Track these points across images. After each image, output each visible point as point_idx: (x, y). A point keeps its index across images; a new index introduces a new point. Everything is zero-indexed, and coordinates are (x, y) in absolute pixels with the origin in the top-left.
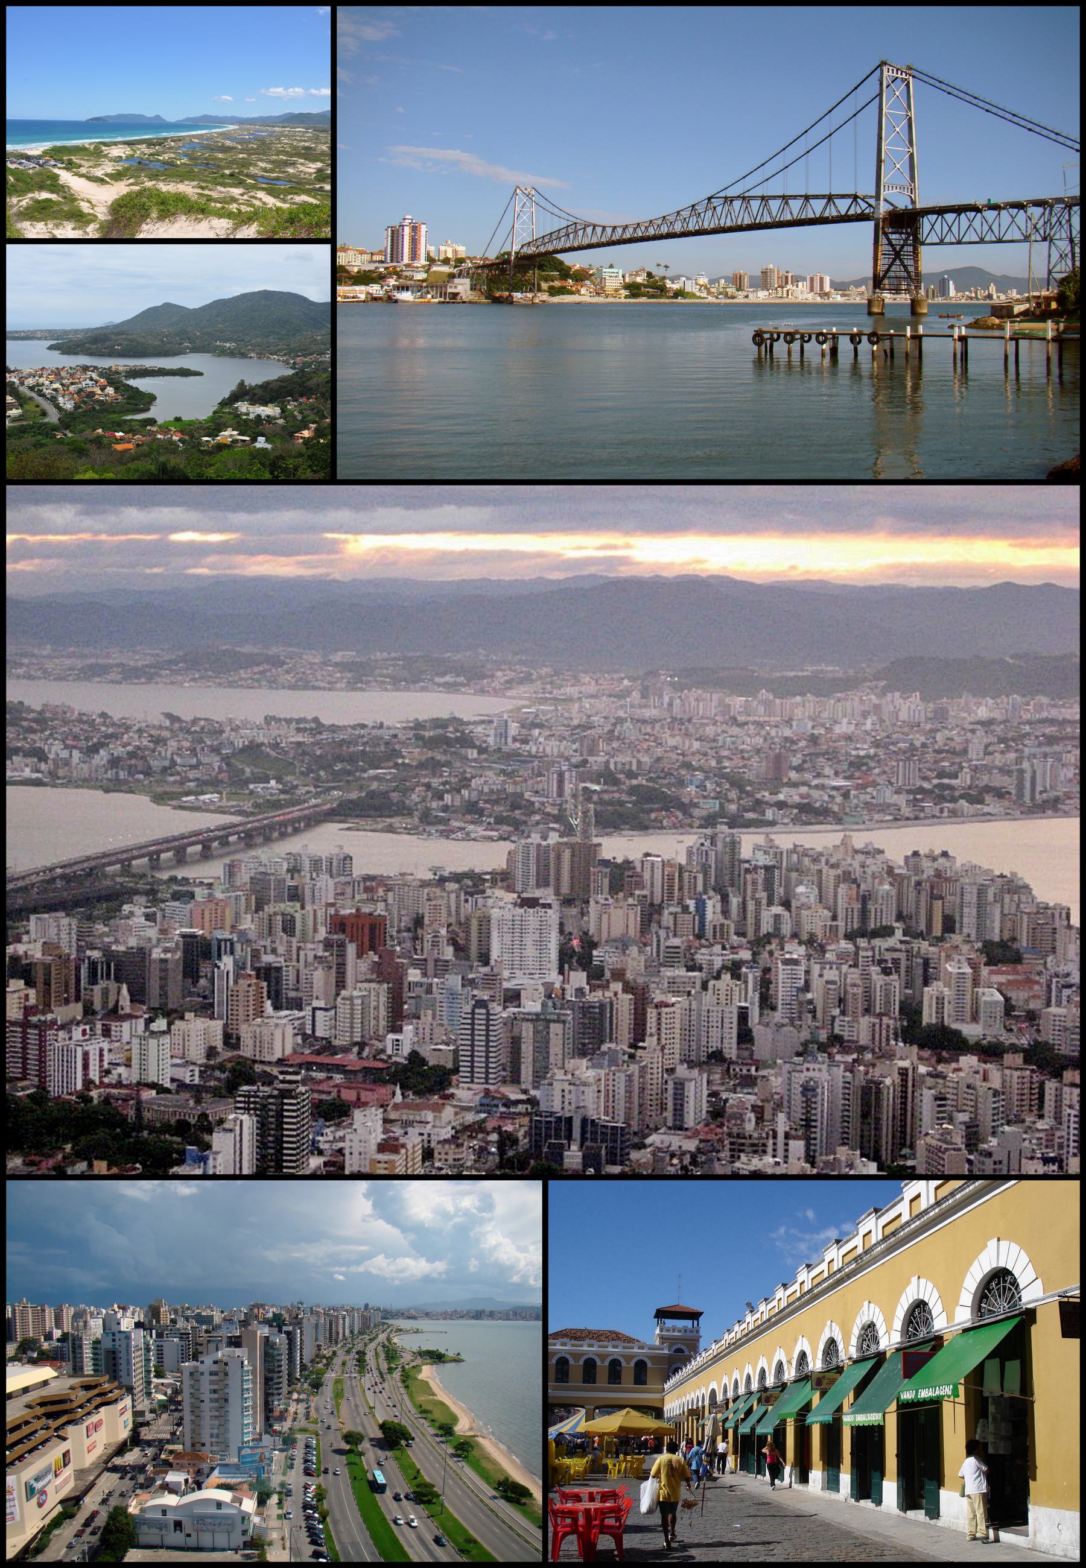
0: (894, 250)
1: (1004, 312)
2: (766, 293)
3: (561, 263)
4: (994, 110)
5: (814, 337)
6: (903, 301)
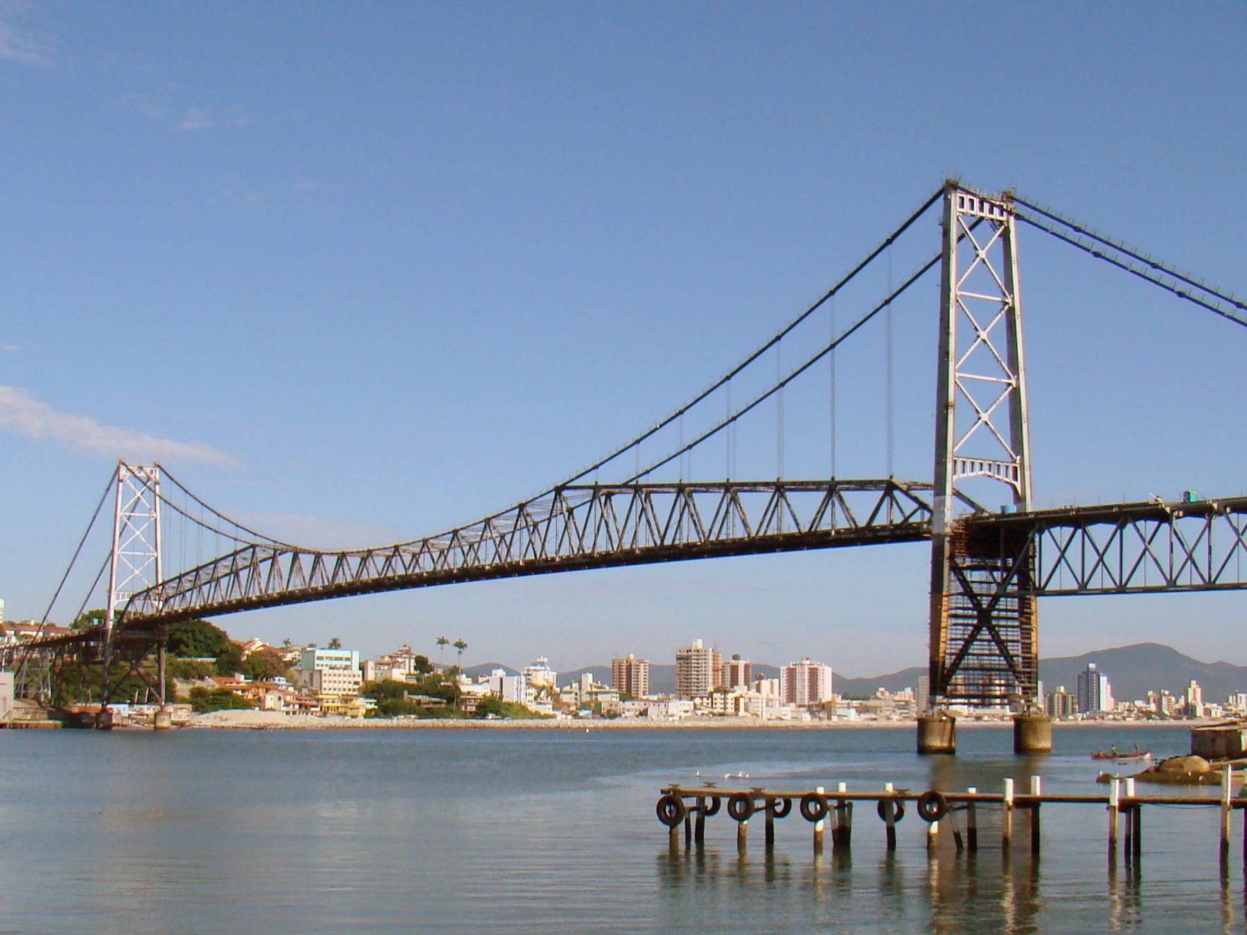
0: (977, 606)
1: (1221, 745)
2: (687, 705)
3: (220, 636)
4: (1196, 293)
5: (796, 804)
6: (997, 722)
